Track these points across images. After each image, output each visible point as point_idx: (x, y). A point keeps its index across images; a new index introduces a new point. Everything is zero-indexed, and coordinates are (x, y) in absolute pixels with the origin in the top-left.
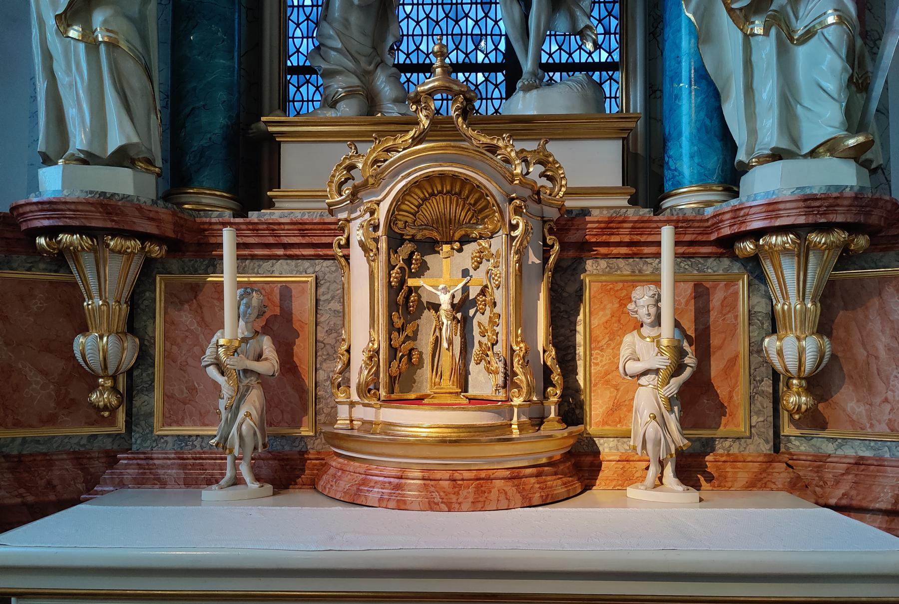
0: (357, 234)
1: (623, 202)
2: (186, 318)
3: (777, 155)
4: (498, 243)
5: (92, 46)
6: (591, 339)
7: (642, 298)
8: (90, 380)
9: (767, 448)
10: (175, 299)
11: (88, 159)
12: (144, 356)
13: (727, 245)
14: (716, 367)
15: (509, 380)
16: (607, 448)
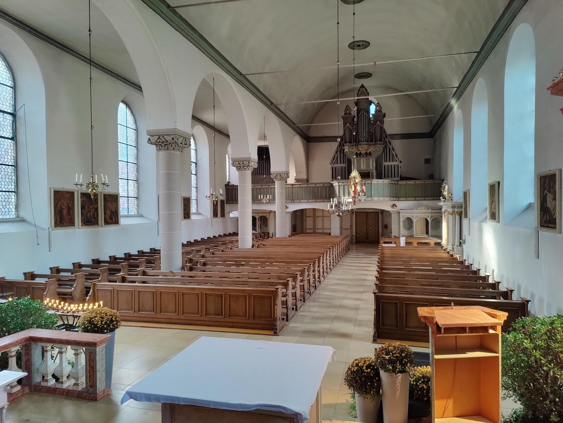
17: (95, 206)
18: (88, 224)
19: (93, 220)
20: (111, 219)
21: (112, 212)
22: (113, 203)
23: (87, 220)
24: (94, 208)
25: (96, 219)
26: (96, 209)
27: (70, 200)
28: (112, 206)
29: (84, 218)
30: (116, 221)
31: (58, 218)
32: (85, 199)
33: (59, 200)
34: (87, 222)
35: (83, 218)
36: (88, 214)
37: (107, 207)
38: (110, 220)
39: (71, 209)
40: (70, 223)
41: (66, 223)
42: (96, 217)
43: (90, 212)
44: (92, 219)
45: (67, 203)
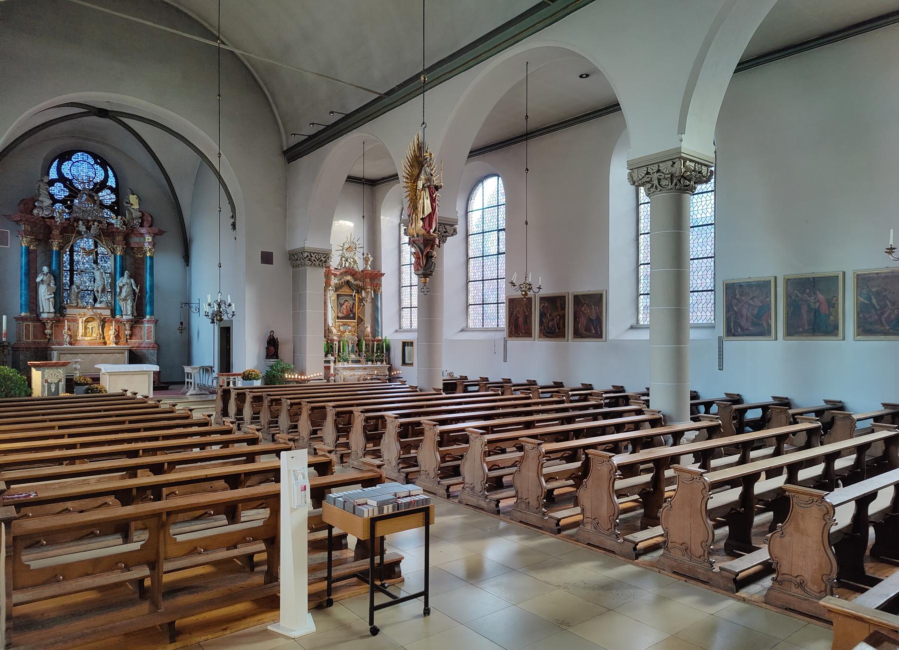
0: (80, 320)
1: (110, 317)
2: (57, 328)
3: (126, 315)
4: (96, 322)
5: (49, 301)
6: (106, 331)
7: (111, 327)
8: (46, 335)
9: (125, 342)
10: (55, 326)
11: (48, 313)
12: (52, 333)
13: (121, 322)
14: (120, 334)
15: (97, 335)
16: (107, 342)
17: (561, 313)
18: (549, 335)
19: (557, 330)
20: (588, 329)
21: (590, 320)
22: (593, 307)
23: (549, 331)
24: (559, 315)
25: (561, 330)
26: (563, 317)
27: (527, 307)
28: (590, 311)
29: (545, 328)
30: (597, 332)
31: (513, 328)
32: (546, 304)
33: (514, 308)
34: (548, 333)
35: (543, 328)
36: (550, 323)
37: (581, 313)
38: (585, 331)
39: (528, 319)
40: (526, 333)
41: (522, 333)
42: (562, 326)
43: (553, 320)
44: (556, 329)
45: (524, 311)
